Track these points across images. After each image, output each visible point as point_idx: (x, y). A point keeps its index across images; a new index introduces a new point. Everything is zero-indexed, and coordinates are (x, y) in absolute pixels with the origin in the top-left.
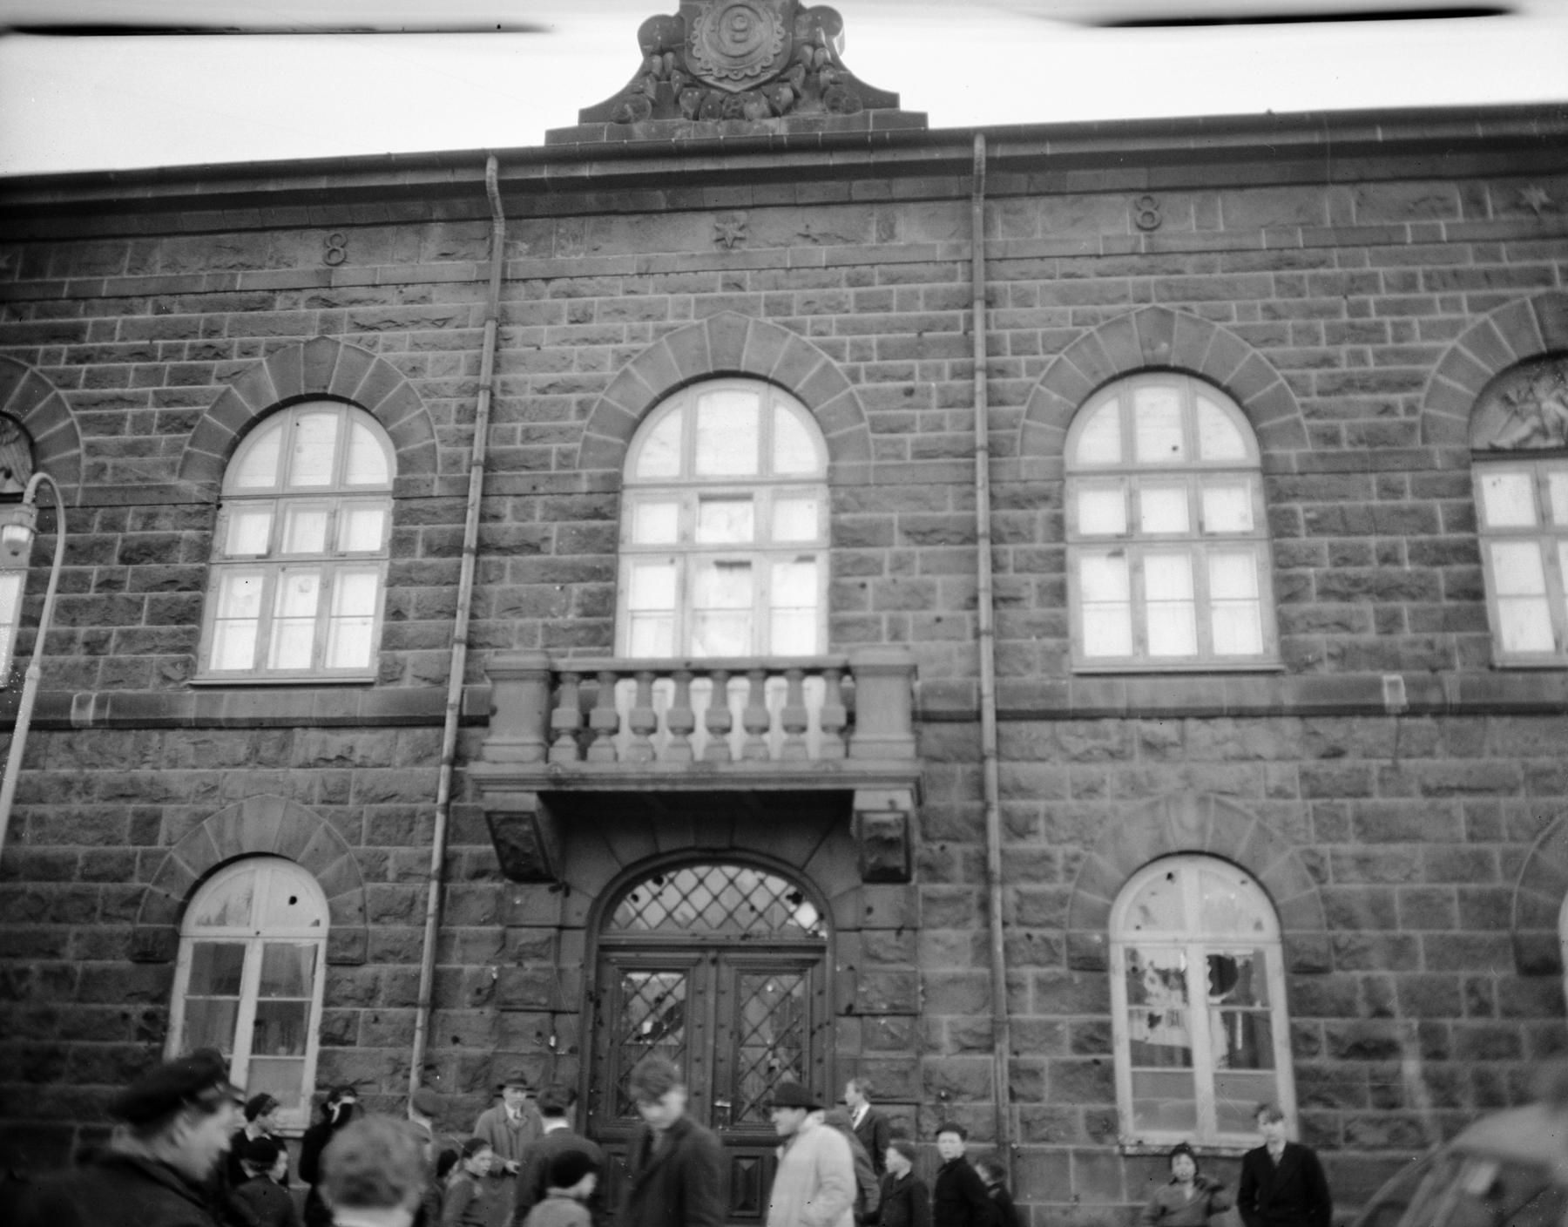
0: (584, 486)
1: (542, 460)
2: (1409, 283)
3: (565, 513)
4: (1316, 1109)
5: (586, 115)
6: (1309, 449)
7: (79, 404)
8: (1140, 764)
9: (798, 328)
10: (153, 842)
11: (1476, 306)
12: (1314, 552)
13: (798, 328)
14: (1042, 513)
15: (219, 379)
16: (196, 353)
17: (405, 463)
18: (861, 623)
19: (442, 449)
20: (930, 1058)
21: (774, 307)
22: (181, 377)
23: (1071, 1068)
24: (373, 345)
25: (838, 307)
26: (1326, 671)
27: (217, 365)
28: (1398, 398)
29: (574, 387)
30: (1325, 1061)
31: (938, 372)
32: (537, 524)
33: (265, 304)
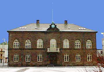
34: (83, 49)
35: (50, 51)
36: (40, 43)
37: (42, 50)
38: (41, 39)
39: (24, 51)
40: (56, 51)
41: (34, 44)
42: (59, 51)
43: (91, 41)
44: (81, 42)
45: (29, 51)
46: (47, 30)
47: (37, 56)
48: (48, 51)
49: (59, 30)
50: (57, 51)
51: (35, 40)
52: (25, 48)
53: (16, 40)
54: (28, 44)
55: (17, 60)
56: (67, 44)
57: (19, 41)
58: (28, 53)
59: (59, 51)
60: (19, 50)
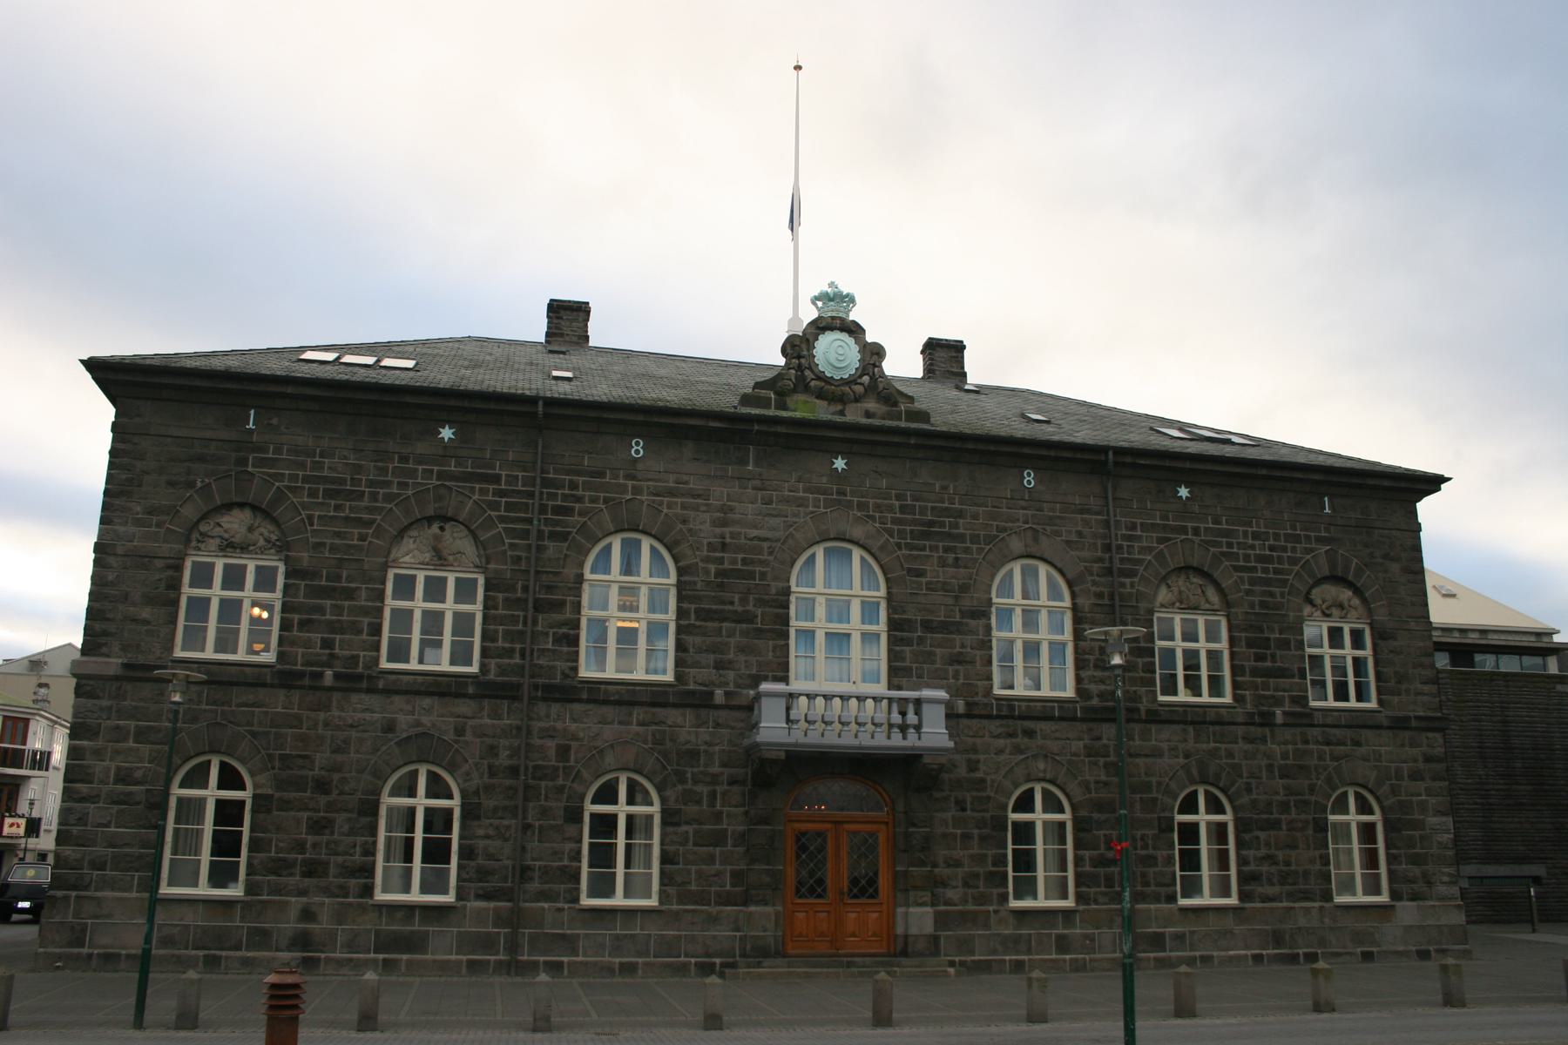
0: (773, 591)
1: (751, 575)
2: (1133, 527)
3: (761, 602)
4: (1084, 889)
5: (758, 385)
6: (1093, 600)
7: (502, 519)
8: (1022, 740)
9: (872, 518)
10: (568, 761)
11: (1160, 541)
12: (1092, 648)
13: (872, 518)
14: (983, 621)
15: (580, 514)
16: (565, 498)
18: (903, 669)
19: (701, 565)
20: (936, 870)
22: (558, 510)
23: (991, 873)
24: (661, 503)
25: (891, 509)
26: (1095, 702)
28: (1127, 581)
29: (766, 539)
31: (937, 547)
32: (750, 607)
33: (601, 474)
34: (1266, 720)
35: (798, 736)
36: (627, 619)
37: (673, 716)
38: (646, 544)
39: (363, 709)
40: (897, 740)
41: (536, 607)
42: (935, 733)
43: (1356, 602)
44: (1227, 604)
45: (433, 716)
46: (746, 400)
47: (575, 816)
48: (772, 727)
49: (923, 416)
50: (912, 740)
51: (552, 548)
52: (385, 664)
53: (235, 523)
54: (433, 619)
55: (222, 875)
56: (1044, 634)
57: (282, 547)
58: (423, 746)
59: (935, 733)
60: (279, 702)
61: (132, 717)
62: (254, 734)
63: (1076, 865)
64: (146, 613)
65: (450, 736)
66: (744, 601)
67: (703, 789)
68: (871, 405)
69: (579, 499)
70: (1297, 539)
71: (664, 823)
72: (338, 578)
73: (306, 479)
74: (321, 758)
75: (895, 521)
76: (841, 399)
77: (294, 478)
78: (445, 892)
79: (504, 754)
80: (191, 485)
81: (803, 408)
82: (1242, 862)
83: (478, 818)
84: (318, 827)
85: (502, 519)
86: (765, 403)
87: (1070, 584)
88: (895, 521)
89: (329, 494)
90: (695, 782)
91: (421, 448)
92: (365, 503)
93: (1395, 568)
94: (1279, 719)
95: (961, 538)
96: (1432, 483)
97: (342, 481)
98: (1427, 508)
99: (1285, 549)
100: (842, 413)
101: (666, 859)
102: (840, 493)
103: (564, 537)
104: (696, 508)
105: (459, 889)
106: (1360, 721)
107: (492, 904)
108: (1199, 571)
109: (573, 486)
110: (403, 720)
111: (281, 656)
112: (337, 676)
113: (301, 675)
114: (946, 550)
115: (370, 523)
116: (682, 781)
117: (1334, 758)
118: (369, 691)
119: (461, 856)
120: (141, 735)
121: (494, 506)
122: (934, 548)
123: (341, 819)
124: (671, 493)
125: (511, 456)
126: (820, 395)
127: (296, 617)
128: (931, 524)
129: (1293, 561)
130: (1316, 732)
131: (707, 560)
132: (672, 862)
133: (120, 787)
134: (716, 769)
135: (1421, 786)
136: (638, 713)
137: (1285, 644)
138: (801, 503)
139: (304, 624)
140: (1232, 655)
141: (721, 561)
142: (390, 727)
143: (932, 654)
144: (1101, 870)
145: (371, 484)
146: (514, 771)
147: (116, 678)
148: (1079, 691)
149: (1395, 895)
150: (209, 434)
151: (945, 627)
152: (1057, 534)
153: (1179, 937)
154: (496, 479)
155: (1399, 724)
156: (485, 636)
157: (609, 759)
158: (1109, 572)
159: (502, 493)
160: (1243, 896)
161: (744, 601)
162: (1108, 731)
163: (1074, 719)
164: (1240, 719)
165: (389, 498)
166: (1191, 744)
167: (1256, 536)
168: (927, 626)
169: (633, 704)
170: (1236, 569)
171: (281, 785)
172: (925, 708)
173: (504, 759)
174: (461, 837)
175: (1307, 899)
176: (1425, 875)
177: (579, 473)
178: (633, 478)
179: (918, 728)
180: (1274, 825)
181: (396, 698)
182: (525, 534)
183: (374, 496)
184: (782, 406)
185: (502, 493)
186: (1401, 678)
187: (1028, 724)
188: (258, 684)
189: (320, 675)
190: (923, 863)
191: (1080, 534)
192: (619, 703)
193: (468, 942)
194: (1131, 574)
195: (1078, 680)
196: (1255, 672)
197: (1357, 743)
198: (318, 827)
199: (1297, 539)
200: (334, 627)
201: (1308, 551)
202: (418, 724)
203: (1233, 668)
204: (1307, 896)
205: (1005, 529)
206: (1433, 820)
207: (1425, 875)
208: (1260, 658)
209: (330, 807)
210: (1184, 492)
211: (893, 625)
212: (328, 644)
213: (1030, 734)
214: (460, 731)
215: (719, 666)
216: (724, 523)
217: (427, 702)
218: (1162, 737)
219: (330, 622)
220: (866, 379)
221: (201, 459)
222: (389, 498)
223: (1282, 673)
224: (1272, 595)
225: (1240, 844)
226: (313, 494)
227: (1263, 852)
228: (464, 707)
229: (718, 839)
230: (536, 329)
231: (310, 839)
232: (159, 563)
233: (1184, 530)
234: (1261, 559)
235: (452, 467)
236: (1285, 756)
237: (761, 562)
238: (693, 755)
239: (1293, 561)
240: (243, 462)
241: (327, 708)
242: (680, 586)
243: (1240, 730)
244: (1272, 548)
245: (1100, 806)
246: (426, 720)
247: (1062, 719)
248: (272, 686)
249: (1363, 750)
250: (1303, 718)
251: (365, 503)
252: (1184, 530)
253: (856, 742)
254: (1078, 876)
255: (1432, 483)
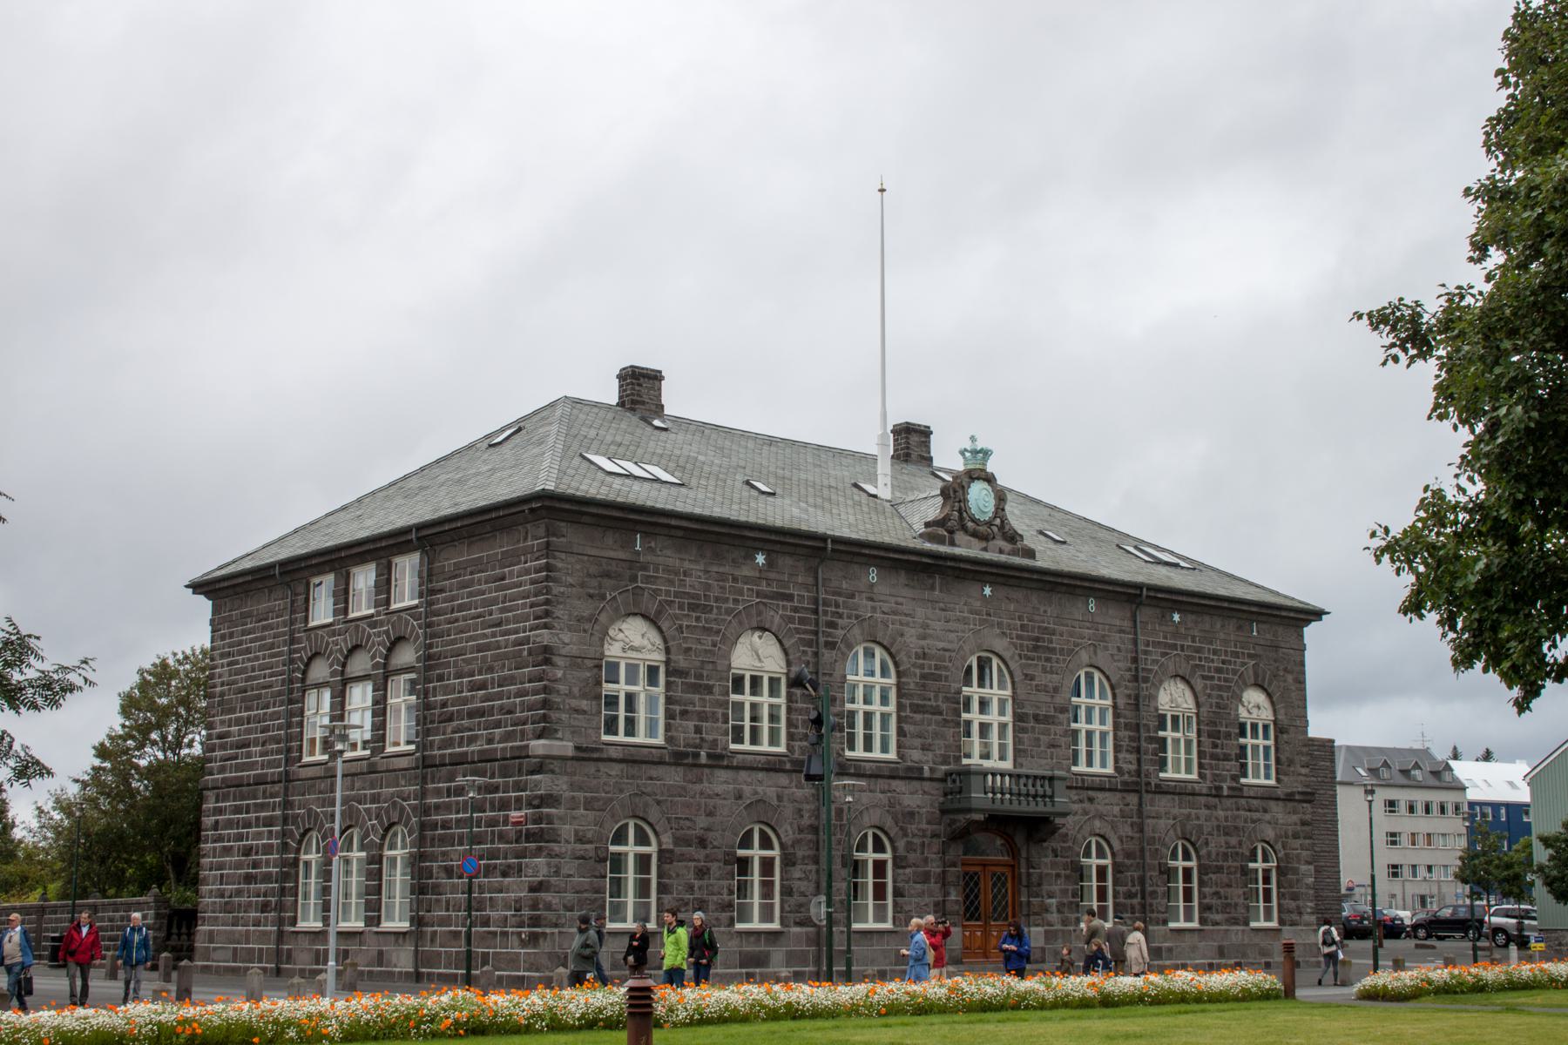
3: (947, 699)
7: (797, 631)
8: (1087, 805)
11: (1164, 654)
17: (899, 674)
18: (1025, 751)
21: (1000, 625)
26: (1126, 777)
27: (840, 621)
30: (1122, 900)
33: (852, 596)
37: (897, 785)
39: (721, 782)
40: (1041, 808)
45: (767, 787)
49: (1031, 554)
50: (1049, 808)
51: (827, 655)
60: (673, 777)
61: (581, 789)
62: (658, 803)
63: (1115, 897)
64: (584, 704)
65: (775, 802)
66: (936, 697)
67: (917, 841)
68: (1001, 543)
69: (841, 616)
70: (1236, 655)
71: (895, 865)
72: (700, 677)
73: (677, 594)
74: (702, 821)
75: (1018, 637)
76: (984, 538)
77: (668, 593)
78: (772, 921)
79: (806, 815)
80: (603, 597)
81: (967, 548)
82: (1202, 896)
83: (794, 864)
84: (702, 873)
85: (797, 631)
86: (941, 540)
87: (1112, 688)
88: (1018, 637)
89: (693, 607)
90: (914, 835)
91: (746, 571)
92: (713, 616)
93: (1290, 678)
94: (1225, 793)
95: (1052, 650)
96: (1318, 614)
97: (697, 597)
98: (1311, 632)
99: (1230, 662)
100: (985, 549)
101: (898, 893)
102: (989, 614)
103: (831, 645)
104: (907, 624)
105: (782, 918)
106: (1267, 795)
107: (804, 929)
108: (1183, 678)
109: (837, 606)
110: (747, 790)
111: (669, 739)
112: (709, 756)
113: (686, 755)
114: (1048, 660)
115: (718, 632)
116: (906, 835)
117: (1253, 821)
118: (727, 767)
119: (782, 894)
120: (588, 805)
121: (791, 620)
122: (1039, 658)
123: (714, 866)
124: (895, 613)
125: (800, 579)
126: (975, 534)
127: (677, 708)
128: (1037, 639)
129: (1235, 672)
130: (1243, 801)
131: (914, 665)
132: (903, 896)
133: (579, 846)
134: (924, 826)
135: (1299, 842)
136: (882, 784)
137: (1228, 736)
138: (965, 621)
139: (684, 713)
140: (1199, 743)
141: (922, 667)
142: (739, 797)
143: (1038, 739)
144: (1129, 901)
145: (717, 599)
146: (815, 829)
147: (573, 758)
148: (1117, 768)
149: (1281, 922)
150: (612, 554)
151: (1047, 720)
152: (1106, 648)
153: (1170, 950)
154: (790, 597)
155: (1289, 798)
156: (790, 724)
157: (866, 820)
158: (1135, 679)
159: (795, 610)
160: (1202, 921)
161: (936, 697)
162: (1133, 799)
163: (1116, 790)
164: (1204, 791)
165: (728, 612)
166: (1176, 811)
167: (1215, 652)
168: (1036, 718)
169: (877, 776)
170: (1204, 677)
171: (678, 841)
172: (1056, 783)
173: (806, 821)
174: (782, 879)
175: (1237, 924)
176: (1298, 907)
177: (840, 594)
178: (871, 599)
179: (1052, 797)
180: (1219, 869)
181: (743, 774)
182: (809, 643)
183: (719, 608)
184: (952, 543)
185: (795, 610)
186: (1291, 762)
187: (1090, 793)
188: (661, 763)
189: (697, 755)
190: (1037, 896)
191: (1119, 649)
192: (871, 776)
193: (791, 958)
194: (1146, 680)
195: (1116, 760)
196: (1214, 757)
197: (1265, 811)
198: (702, 873)
199: (1236, 655)
200: (703, 717)
201: (1243, 664)
202: (756, 793)
203: (1199, 752)
204: (1235, 922)
205: (1076, 645)
206: (1304, 868)
207: (1298, 907)
208: (1215, 746)
209: (708, 858)
210: (1176, 617)
211: (1019, 718)
212: (698, 730)
213: (1091, 800)
214: (780, 798)
215: (924, 748)
216: (924, 638)
217: (760, 775)
218: (1163, 804)
219: (699, 713)
220: (998, 521)
221: (607, 575)
222: (728, 612)
223: (1227, 758)
224: (1221, 697)
225: (1201, 883)
226: (681, 607)
227: (1214, 889)
228: (783, 779)
229: (925, 878)
230: (610, 394)
231: (697, 883)
232: (589, 663)
233: (1174, 647)
234: (1219, 670)
235: (764, 587)
236: (1226, 819)
237: (946, 668)
238: (912, 814)
239: (1235, 672)
240: (634, 579)
241: (701, 781)
242: (899, 686)
243: (1203, 800)
244: (1224, 662)
245: (1128, 855)
246: (760, 789)
247: (1110, 790)
248: (669, 764)
249: (1267, 817)
250: (1238, 792)
251: (713, 616)
252: (1174, 647)
253: (1002, 807)
254: (1116, 905)
255: (1318, 614)
